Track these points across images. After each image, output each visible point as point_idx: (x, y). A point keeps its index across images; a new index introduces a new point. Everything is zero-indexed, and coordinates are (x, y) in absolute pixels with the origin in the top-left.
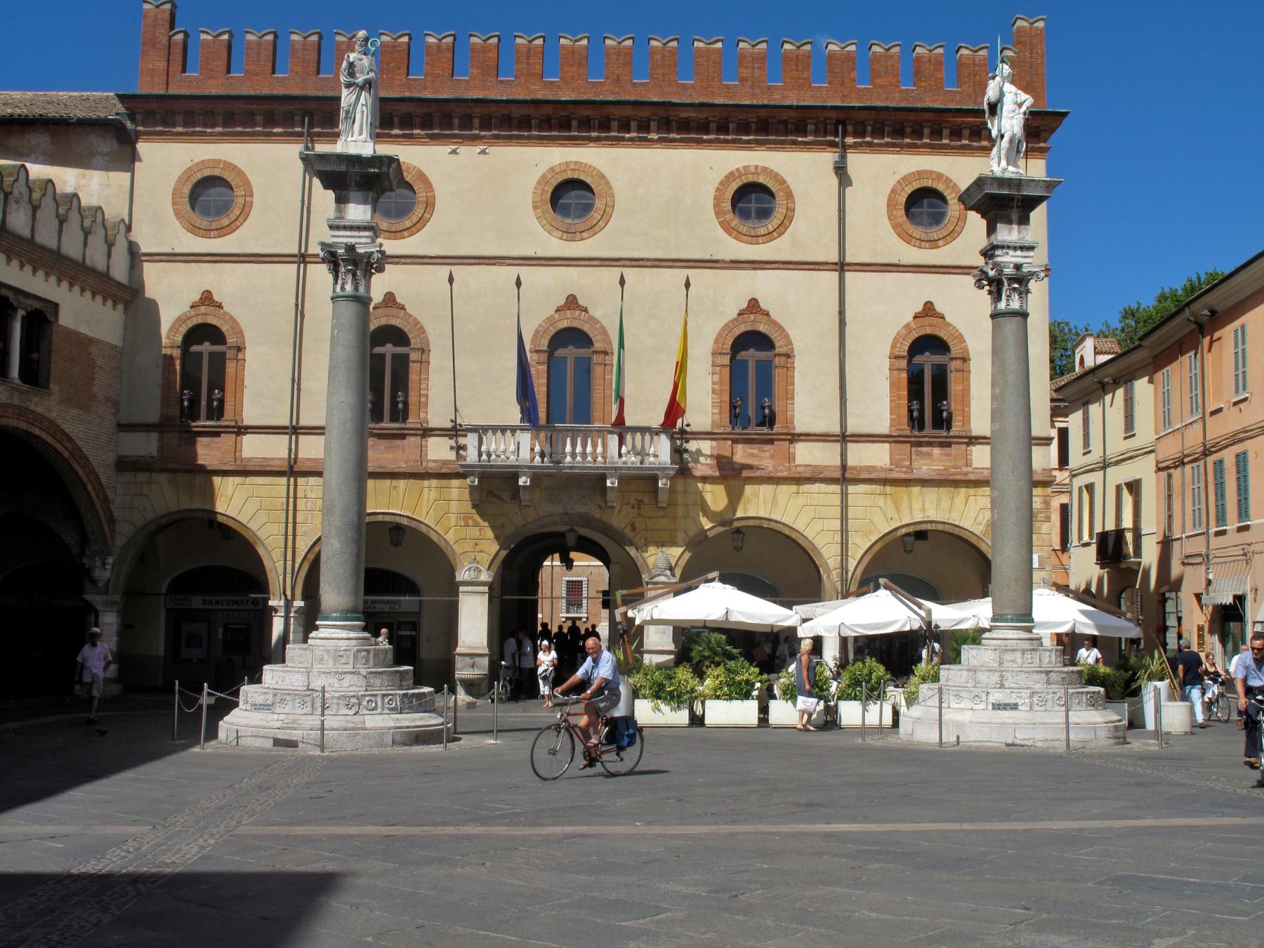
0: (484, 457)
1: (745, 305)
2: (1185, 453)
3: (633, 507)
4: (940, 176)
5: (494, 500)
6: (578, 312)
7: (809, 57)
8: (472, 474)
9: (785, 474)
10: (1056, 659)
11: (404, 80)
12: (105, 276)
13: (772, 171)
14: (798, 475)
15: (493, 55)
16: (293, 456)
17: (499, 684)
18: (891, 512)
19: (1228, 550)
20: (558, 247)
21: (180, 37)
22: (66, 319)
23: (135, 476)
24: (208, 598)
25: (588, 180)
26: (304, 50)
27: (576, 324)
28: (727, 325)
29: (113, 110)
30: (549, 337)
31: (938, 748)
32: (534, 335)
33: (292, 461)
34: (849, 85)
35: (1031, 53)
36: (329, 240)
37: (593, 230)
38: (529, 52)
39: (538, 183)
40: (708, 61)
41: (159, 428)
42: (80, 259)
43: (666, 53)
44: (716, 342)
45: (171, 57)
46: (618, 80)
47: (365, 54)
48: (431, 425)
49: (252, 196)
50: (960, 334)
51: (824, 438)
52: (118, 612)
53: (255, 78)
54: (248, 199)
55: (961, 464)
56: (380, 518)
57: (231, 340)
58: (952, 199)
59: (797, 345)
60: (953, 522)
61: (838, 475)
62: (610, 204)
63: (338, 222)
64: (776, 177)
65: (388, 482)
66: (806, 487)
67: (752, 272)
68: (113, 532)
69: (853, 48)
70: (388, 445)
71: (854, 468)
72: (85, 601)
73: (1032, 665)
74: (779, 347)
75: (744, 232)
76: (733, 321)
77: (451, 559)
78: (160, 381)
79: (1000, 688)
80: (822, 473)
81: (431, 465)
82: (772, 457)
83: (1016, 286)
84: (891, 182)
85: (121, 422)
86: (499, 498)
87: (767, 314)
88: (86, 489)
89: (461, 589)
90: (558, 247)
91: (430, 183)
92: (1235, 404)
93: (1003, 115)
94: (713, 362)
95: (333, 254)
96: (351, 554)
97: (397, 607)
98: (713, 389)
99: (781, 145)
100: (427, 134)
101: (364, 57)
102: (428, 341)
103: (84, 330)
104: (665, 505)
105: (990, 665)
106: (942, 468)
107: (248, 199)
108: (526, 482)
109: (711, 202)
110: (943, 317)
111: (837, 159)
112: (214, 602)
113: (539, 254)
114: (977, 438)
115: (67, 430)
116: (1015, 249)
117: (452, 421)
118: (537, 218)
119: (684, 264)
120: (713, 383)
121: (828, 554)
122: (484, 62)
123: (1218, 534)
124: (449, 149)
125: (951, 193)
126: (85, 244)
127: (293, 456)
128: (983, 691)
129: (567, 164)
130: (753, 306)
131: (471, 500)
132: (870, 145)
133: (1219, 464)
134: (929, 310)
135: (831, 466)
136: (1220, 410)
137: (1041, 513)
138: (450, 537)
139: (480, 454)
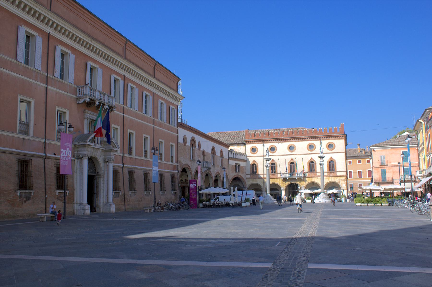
1: (311, 158)
4: (332, 142)
12: (244, 160)
18: (328, 180)
21: (249, 133)
22: (241, 165)
37: (294, 151)
41: (250, 175)
64: (314, 144)
66: (318, 178)
78: (250, 170)
82: (314, 175)
84: (326, 144)
87: (313, 159)
99: (314, 140)
110: (333, 158)
124: (278, 143)
130: (312, 158)
132: (324, 139)
134: (331, 158)
138: (281, 185)
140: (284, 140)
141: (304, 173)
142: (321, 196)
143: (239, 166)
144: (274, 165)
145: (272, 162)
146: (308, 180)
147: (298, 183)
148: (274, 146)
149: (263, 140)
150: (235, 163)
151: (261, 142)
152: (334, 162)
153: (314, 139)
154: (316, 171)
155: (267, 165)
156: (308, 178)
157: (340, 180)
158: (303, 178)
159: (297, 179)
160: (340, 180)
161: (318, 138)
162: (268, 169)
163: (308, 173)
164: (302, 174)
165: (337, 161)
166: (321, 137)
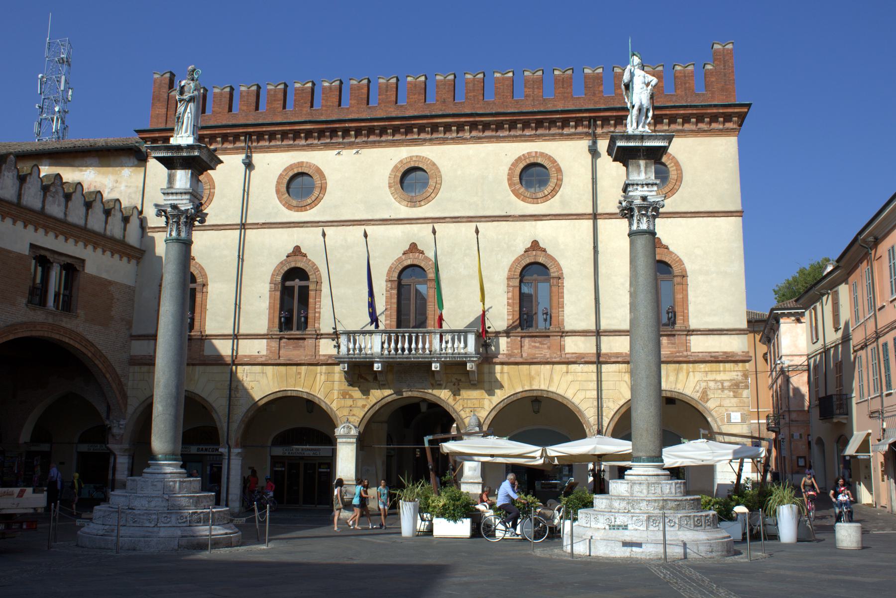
0: (351, 352)
1: (529, 246)
2: (867, 338)
3: (454, 385)
5: (362, 380)
6: (417, 254)
7: (571, 78)
8: (344, 362)
9: (557, 360)
10: (676, 490)
11: (309, 111)
13: (547, 154)
14: (567, 360)
15: (365, 91)
16: (235, 354)
17: (55, 507)
19: (894, 407)
20: (404, 211)
22: (90, 269)
23: (140, 368)
24: (201, 447)
25: (425, 168)
26: (248, 96)
27: (416, 262)
28: (517, 259)
29: (134, 139)
30: (398, 271)
31: (570, 559)
32: (389, 270)
33: (234, 357)
34: (598, 95)
35: (724, 66)
36: (162, 202)
37: (427, 199)
38: (387, 87)
39: (392, 171)
40: (503, 85)
42: (102, 231)
43: (476, 82)
44: (510, 270)
45: (169, 106)
46: (444, 102)
47: (193, 80)
48: (322, 332)
49: (214, 188)
50: (680, 259)
51: (585, 334)
52: (129, 455)
53: (218, 115)
54: (212, 190)
55: (682, 350)
56: (289, 394)
57: (199, 280)
58: (672, 167)
59: (566, 271)
60: (678, 391)
61: (594, 359)
62: (438, 182)
63: (170, 191)
65: (294, 367)
67: (534, 223)
68: (126, 404)
69: (600, 70)
70: (294, 345)
71: (606, 354)
72: (108, 449)
73: (656, 495)
74: (553, 273)
75: (528, 196)
76: (521, 256)
77: (335, 421)
79: (627, 513)
80: (584, 358)
81: (322, 358)
82: (549, 348)
83: (644, 212)
85: (133, 334)
86: (367, 380)
87: (544, 250)
88: (106, 378)
89: (339, 440)
90: (404, 211)
91: (324, 175)
92: (891, 302)
93: (634, 92)
94: (508, 284)
95: (165, 211)
96: (170, 415)
97: (318, 453)
98: (508, 302)
99: (553, 137)
100: (322, 143)
101: (192, 82)
102: (321, 276)
103: (104, 276)
104: (476, 382)
105: (625, 495)
106: (669, 353)
107: (212, 190)
108: (378, 368)
109: (505, 177)
110: (667, 248)
111: (591, 144)
112: (204, 449)
113: (392, 217)
114: (693, 331)
115: (90, 339)
116: (642, 185)
117: (334, 329)
118: (392, 194)
119: (487, 219)
120: (508, 299)
121: (589, 414)
122: (358, 96)
123: (888, 395)
124: (336, 152)
125: (671, 163)
126: (106, 222)
127: (235, 354)
128: (612, 515)
129: (411, 157)
130: (535, 245)
131: (348, 381)
133: (885, 345)
135: (590, 353)
136: (883, 307)
137: (742, 383)
138: (334, 406)
139: (349, 350)
140: (371, 131)
141: (485, 338)
142: (637, 488)
143: (72, 268)
144: (303, 283)
145: (293, 265)
146: (506, 376)
147: (444, 395)
148: (309, 165)
149: (245, 134)
150: (32, 246)
151: (238, 144)
152: (676, 270)
153: (554, 131)
154: (561, 323)
155: (173, 200)
156: (506, 367)
157: (712, 385)
158: (479, 365)
159: (435, 367)
160: (712, 384)
161: (579, 122)
162: (178, 240)
163: (507, 333)
164: (471, 339)
165: (689, 267)
166: (595, 119)
